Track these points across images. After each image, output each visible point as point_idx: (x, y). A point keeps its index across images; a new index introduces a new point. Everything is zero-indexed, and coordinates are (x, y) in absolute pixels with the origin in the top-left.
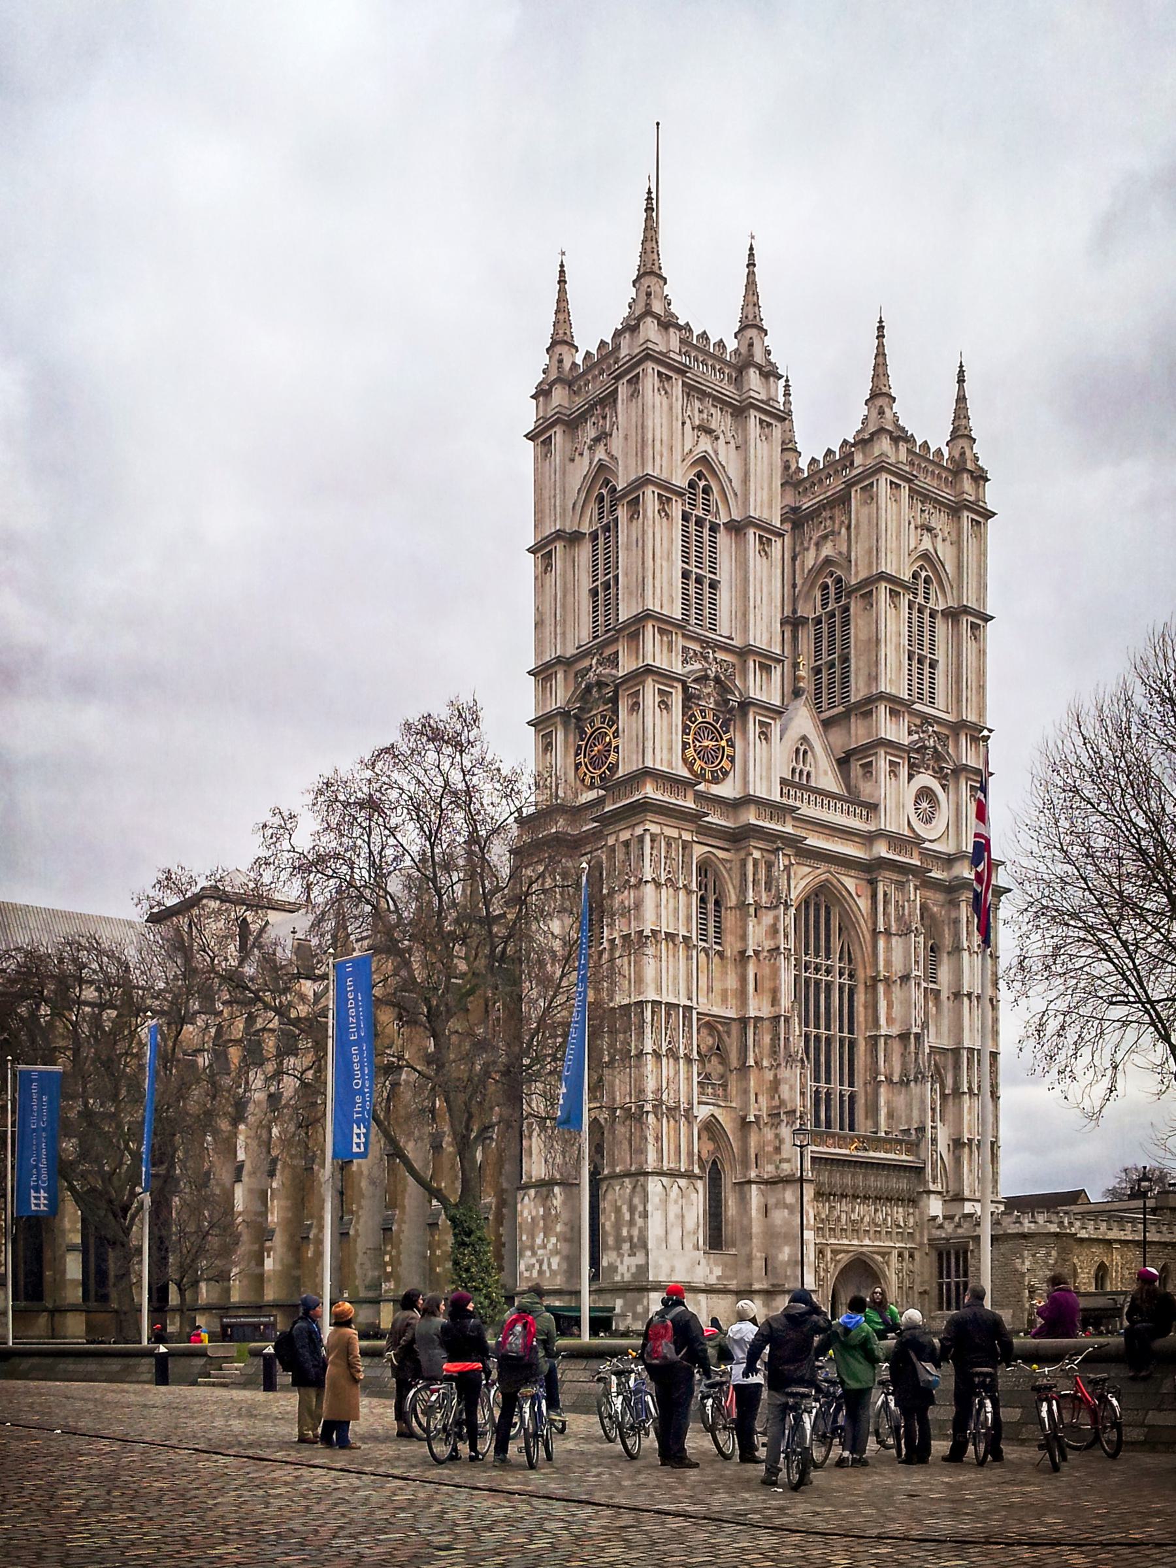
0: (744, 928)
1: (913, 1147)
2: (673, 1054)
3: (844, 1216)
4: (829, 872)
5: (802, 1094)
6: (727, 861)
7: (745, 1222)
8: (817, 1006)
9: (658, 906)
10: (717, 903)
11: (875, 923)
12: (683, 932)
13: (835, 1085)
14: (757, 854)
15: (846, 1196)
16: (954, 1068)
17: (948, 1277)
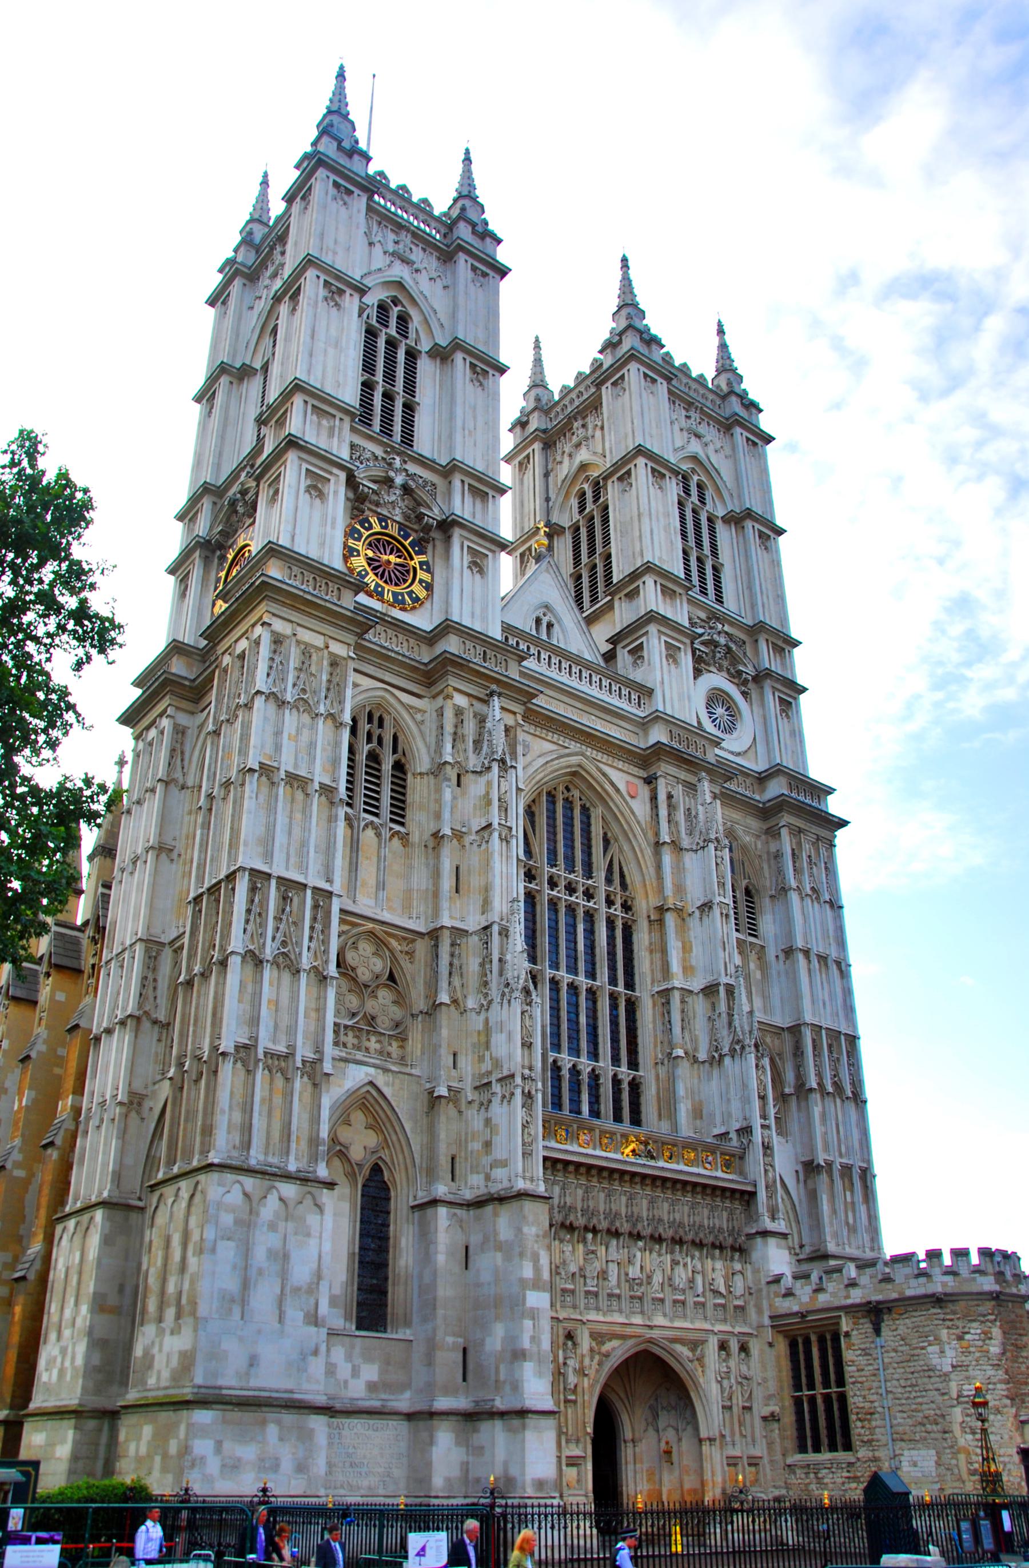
0: (439, 801)
1: (735, 1160)
2: (286, 962)
3: (613, 1269)
4: (583, 754)
5: (527, 1045)
6: (420, 711)
7: (427, 1280)
8: (572, 940)
9: (278, 733)
10: (399, 767)
11: (657, 834)
12: (320, 776)
13: (605, 1063)
14: (461, 700)
15: (617, 1234)
16: (795, 1055)
17: (811, 1386)
